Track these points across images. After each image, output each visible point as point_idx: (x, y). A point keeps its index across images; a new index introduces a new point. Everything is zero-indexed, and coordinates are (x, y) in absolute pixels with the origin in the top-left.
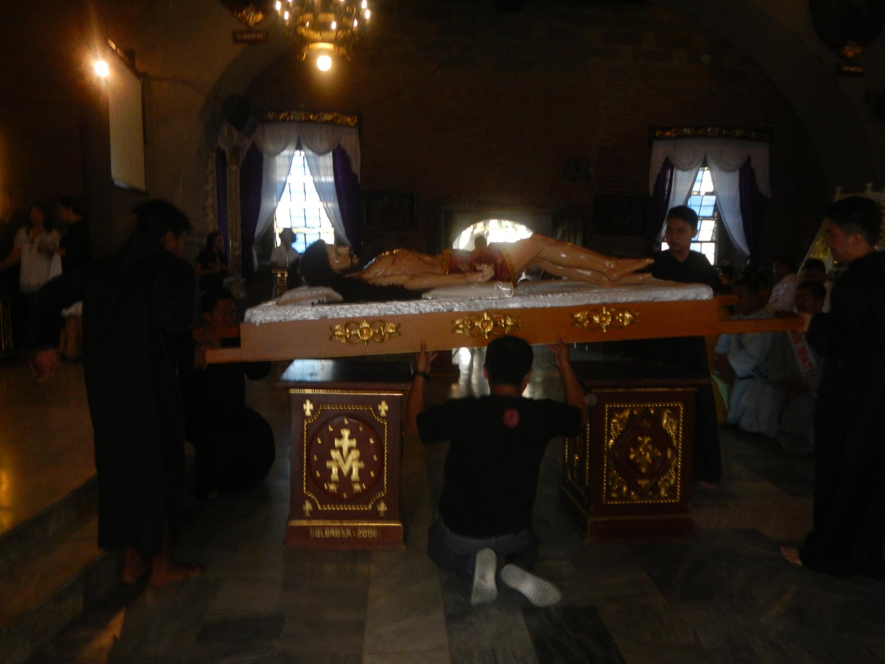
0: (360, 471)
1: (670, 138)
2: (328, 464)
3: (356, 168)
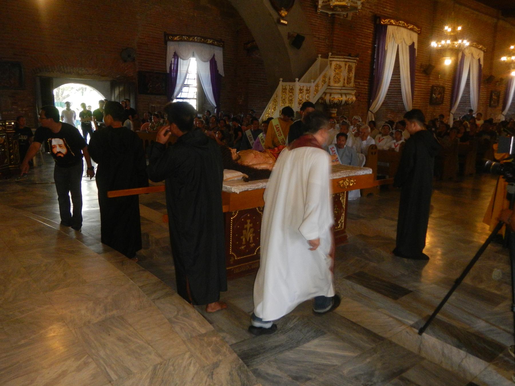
1: (176, 41)
2: (242, 237)
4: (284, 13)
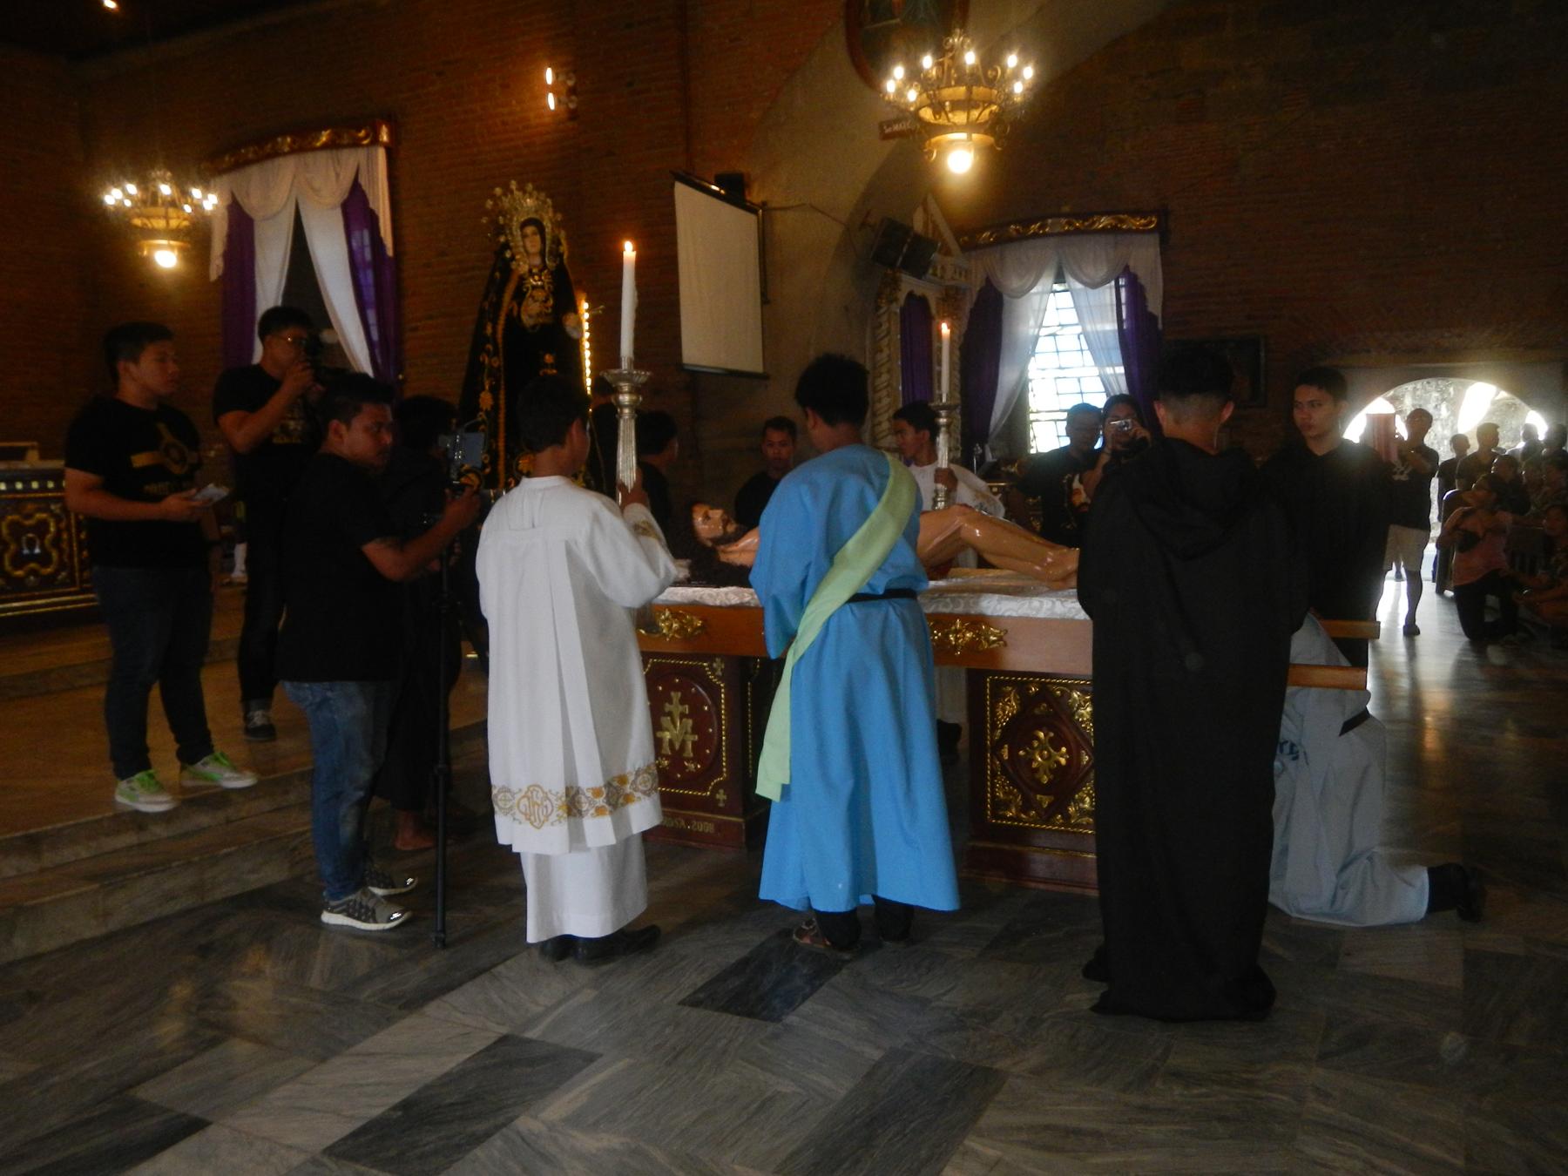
0: (694, 743)
3: (1155, 305)
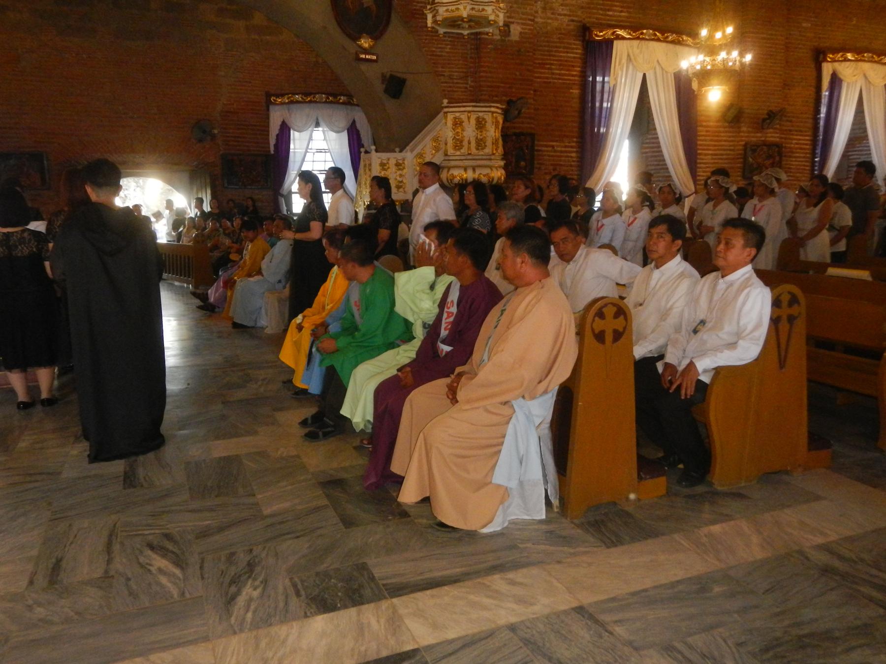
1: (282, 104)
4: (365, 43)
